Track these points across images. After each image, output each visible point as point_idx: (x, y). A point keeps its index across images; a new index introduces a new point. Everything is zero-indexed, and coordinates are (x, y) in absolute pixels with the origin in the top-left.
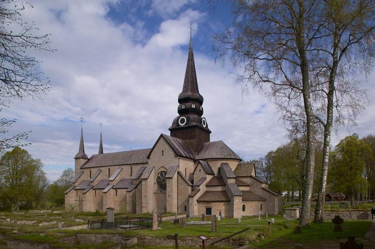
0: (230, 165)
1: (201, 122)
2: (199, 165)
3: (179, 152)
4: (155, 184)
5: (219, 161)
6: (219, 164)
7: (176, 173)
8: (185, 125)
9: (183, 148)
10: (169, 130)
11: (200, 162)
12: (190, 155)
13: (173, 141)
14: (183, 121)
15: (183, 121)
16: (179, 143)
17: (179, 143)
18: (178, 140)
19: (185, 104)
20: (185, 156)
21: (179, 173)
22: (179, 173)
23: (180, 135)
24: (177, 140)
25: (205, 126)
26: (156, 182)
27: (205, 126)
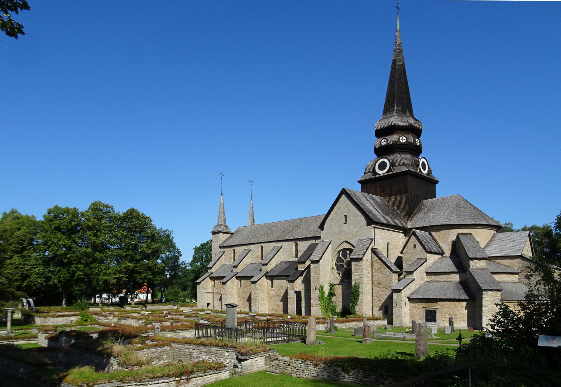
0: (475, 236)
1: (418, 165)
2: (413, 237)
3: (376, 217)
4: (333, 269)
5: (453, 230)
6: (453, 234)
7: (370, 251)
8: (387, 172)
9: (382, 210)
10: (359, 182)
11: (414, 232)
12: (397, 221)
13: (364, 201)
14: (383, 166)
15: (383, 166)
16: (375, 202)
17: (375, 202)
18: (375, 197)
19: (387, 137)
20: (385, 222)
21: (374, 252)
22: (374, 252)
23: (379, 190)
24: (374, 200)
25: (425, 172)
26: (334, 266)
27: (425, 172)
